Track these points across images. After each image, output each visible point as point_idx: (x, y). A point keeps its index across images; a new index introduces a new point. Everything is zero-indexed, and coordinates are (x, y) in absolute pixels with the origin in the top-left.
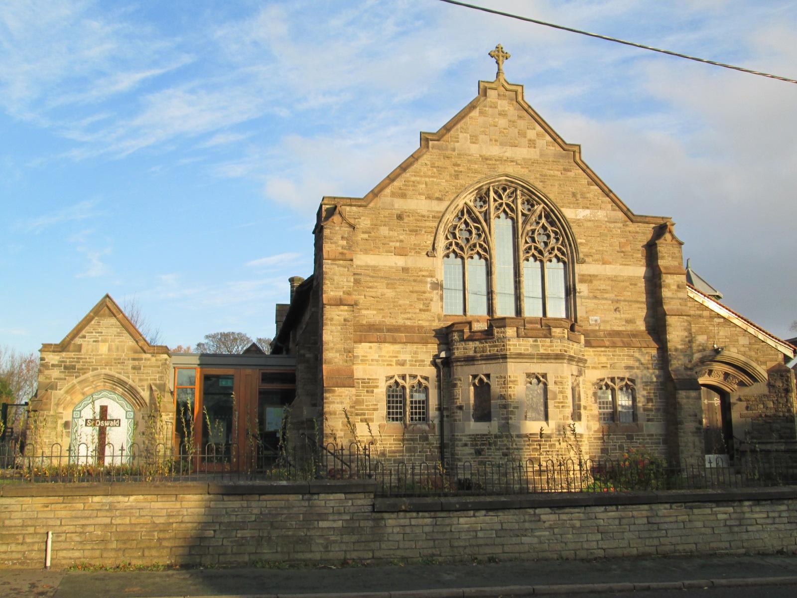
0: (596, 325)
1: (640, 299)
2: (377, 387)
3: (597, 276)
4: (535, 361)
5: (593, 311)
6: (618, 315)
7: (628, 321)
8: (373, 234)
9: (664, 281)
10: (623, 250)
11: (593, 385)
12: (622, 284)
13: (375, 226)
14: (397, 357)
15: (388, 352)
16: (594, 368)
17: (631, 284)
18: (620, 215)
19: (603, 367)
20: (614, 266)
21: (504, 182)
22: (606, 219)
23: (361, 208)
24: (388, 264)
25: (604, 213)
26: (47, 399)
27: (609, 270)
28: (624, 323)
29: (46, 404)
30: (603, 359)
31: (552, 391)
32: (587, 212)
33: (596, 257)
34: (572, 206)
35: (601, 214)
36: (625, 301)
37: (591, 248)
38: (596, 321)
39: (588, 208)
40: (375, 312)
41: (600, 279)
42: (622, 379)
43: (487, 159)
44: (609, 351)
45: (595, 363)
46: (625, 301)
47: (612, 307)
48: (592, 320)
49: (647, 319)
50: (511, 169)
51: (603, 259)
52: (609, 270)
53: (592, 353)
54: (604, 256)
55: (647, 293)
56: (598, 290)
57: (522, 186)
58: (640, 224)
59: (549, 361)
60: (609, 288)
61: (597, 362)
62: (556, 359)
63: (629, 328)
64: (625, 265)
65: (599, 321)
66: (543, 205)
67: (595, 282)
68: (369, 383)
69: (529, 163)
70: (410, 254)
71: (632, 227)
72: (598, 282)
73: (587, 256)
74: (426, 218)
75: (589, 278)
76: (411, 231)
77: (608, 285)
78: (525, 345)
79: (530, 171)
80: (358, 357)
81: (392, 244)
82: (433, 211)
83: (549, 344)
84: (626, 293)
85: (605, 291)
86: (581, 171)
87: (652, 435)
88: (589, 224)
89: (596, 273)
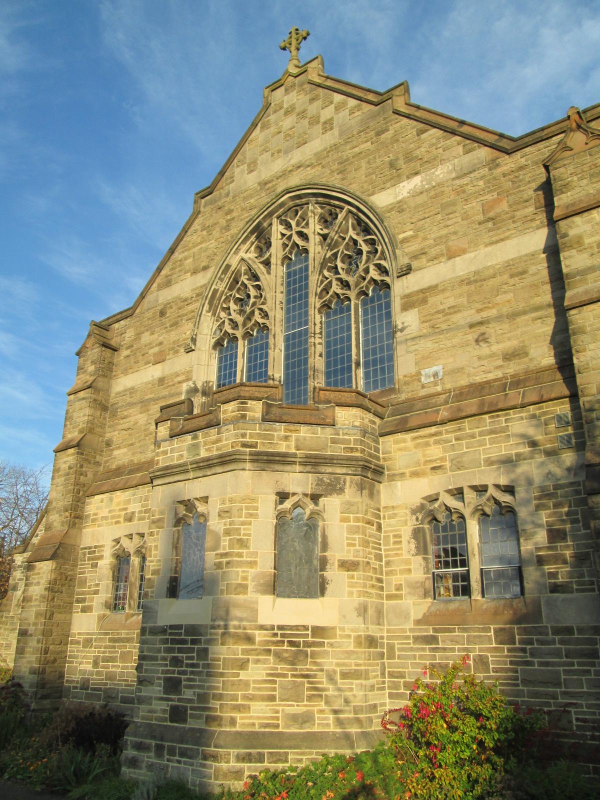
0: (436, 384)
1: (537, 301)
2: (101, 557)
3: (437, 286)
4: (191, 475)
5: (425, 360)
6: (484, 350)
7: (509, 356)
8: (135, 347)
9: (565, 235)
10: (491, 214)
11: (414, 512)
12: (491, 282)
13: (138, 335)
14: (126, 509)
15: (119, 504)
16: (415, 474)
17: (512, 276)
18: (484, 153)
19: (433, 468)
20: (472, 255)
21: (291, 203)
22: (454, 175)
23: (128, 319)
24: (145, 380)
25: (452, 161)
26: (7, 600)
27: (462, 266)
28: (500, 362)
29: (6, 605)
30: (435, 452)
31: (213, 532)
32: (417, 180)
33: (433, 252)
34: (388, 185)
35: (441, 172)
36: (499, 318)
37: (425, 239)
38: (435, 375)
39: (416, 174)
40: (125, 450)
41: (443, 291)
42: (481, 490)
43: (266, 184)
44: (447, 432)
45: (418, 463)
46: (499, 318)
47: (471, 336)
48: (428, 376)
49: (558, 338)
50: (295, 180)
51: (448, 250)
52: (462, 266)
53: (410, 444)
54: (450, 243)
55: (551, 282)
56: (438, 312)
57: (314, 195)
58: (527, 149)
59: (214, 470)
60: (464, 300)
61: (422, 460)
62: (223, 463)
63: (513, 368)
64: (497, 242)
65: (441, 374)
66: (347, 207)
67: (431, 300)
68: (94, 552)
69: (320, 159)
70: (168, 357)
71: (508, 163)
72: (440, 297)
73: (415, 257)
74: (189, 301)
75: (421, 296)
76: (171, 326)
77: (461, 295)
78: (179, 449)
79: (323, 167)
80: (89, 516)
81: (151, 351)
82: (197, 288)
83: (214, 438)
84: (500, 299)
85: (455, 309)
86: (406, 120)
87: (569, 630)
88: (420, 200)
89: (434, 283)
